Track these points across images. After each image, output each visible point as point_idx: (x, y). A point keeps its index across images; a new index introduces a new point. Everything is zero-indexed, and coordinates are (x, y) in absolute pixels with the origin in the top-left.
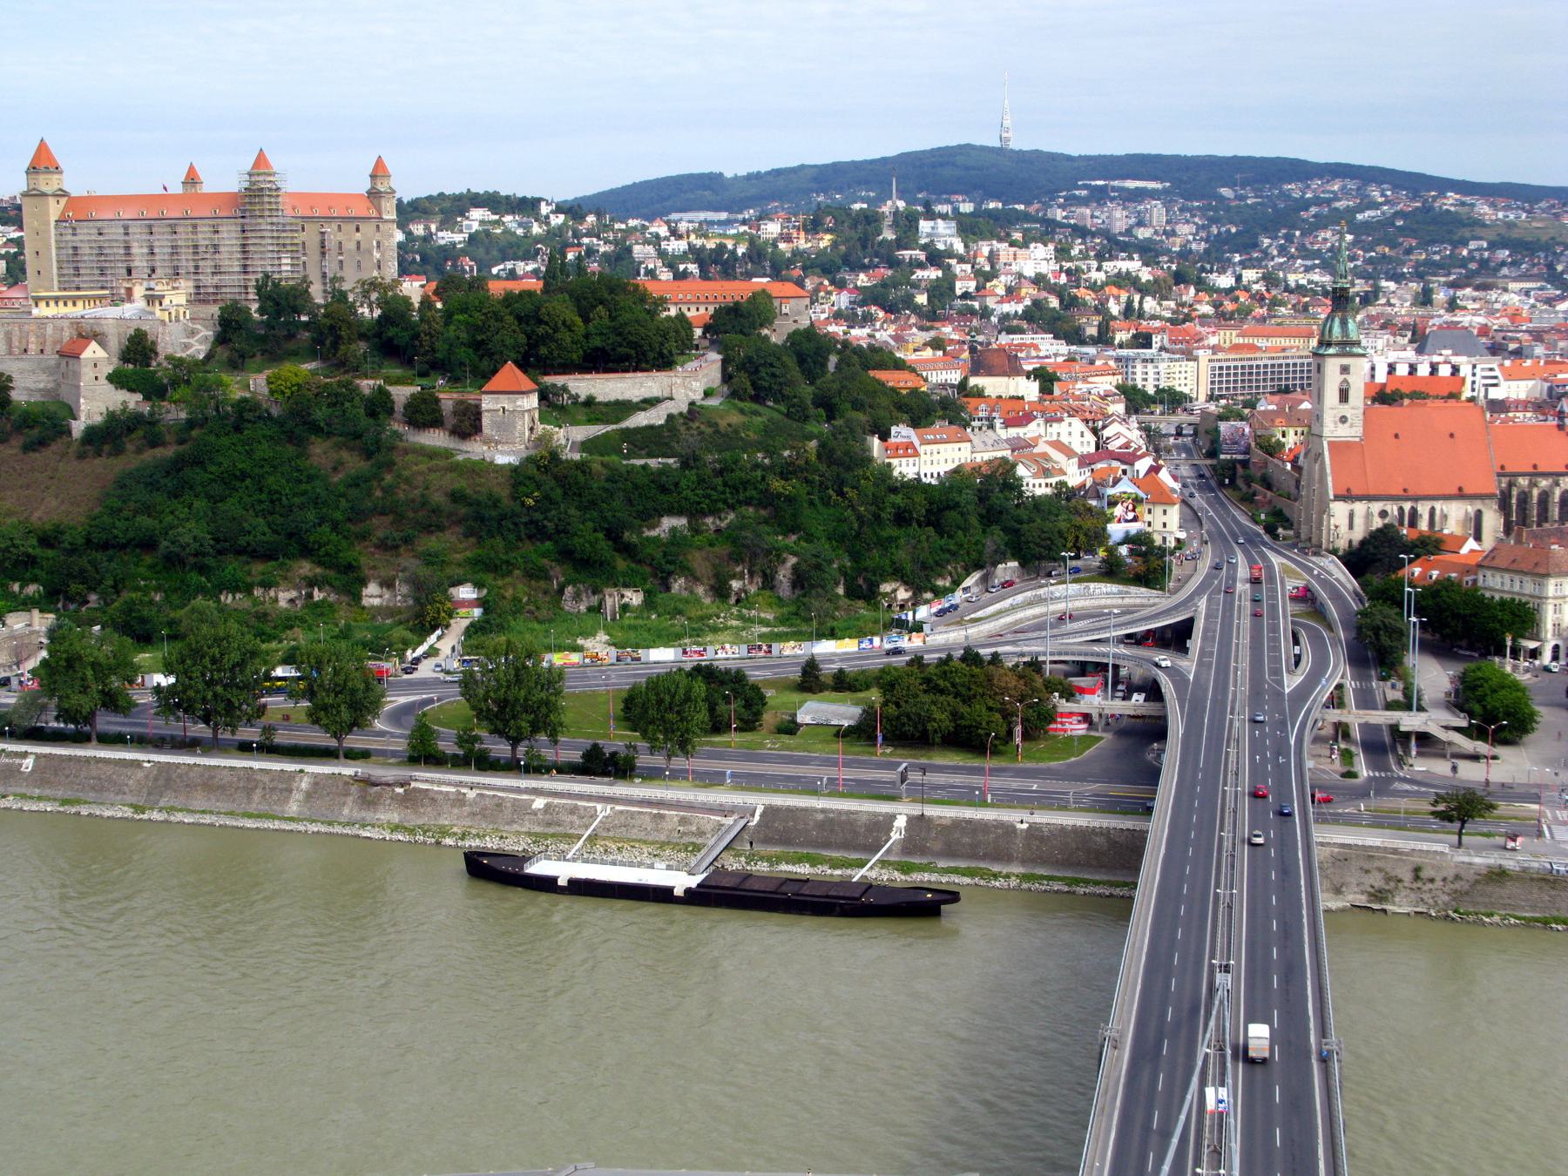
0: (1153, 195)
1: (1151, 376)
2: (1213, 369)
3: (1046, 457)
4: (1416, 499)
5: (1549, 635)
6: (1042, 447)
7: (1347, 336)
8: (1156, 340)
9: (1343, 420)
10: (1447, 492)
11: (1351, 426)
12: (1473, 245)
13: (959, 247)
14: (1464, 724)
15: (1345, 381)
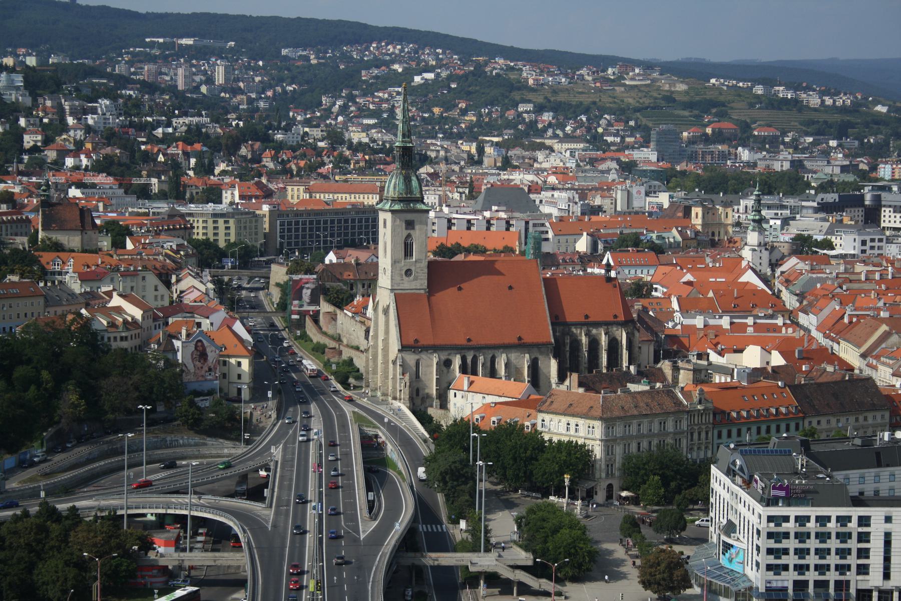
0: (220, 54)
1: (222, 231)
2: (282, 224)
3: (119, 310)
4: (479, 348)
5: (603, 475)
6: (116, 301)
7: (411, 192)
8: (227, 197)
9: (408, 272)
10: (506, 341)
11: (416, 279)
12: (521, 108)
13: (28, 101)
14: (530, 563)
15: (409, 236)
